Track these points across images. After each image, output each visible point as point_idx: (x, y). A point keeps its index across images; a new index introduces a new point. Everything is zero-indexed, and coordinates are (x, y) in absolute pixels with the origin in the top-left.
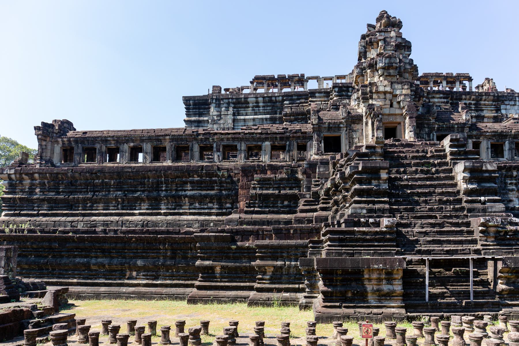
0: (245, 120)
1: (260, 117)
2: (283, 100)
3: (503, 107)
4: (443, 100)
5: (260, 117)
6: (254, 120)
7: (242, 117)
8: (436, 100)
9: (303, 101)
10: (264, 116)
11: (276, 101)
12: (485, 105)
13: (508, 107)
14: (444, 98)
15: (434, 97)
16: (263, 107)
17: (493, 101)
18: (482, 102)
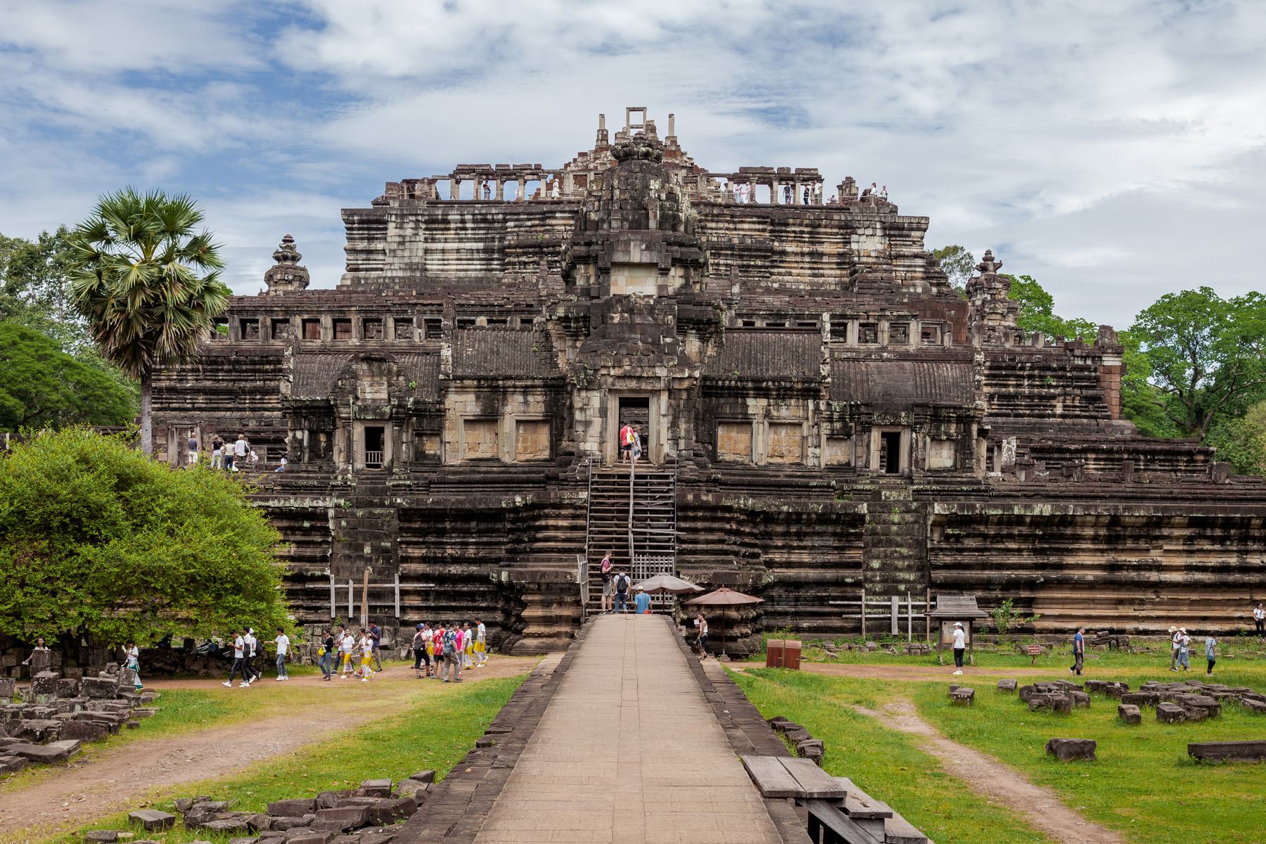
0: (443, 251)
1: (468, 245)
2: (506, 221)
3: (854, 237)
4: (757, 226)
5: (468, 245)
6: (458, 251)
7: (439, 246)
8: (746, 226)
9: (537, 222)
10: (475, 245)
11: (494, 221)
12: (826, 233)
13: (863, 238)
14: (759, 223)
15: (742, 222)
16: (473, 229)
17: (840, 227)
18: (822, 230)
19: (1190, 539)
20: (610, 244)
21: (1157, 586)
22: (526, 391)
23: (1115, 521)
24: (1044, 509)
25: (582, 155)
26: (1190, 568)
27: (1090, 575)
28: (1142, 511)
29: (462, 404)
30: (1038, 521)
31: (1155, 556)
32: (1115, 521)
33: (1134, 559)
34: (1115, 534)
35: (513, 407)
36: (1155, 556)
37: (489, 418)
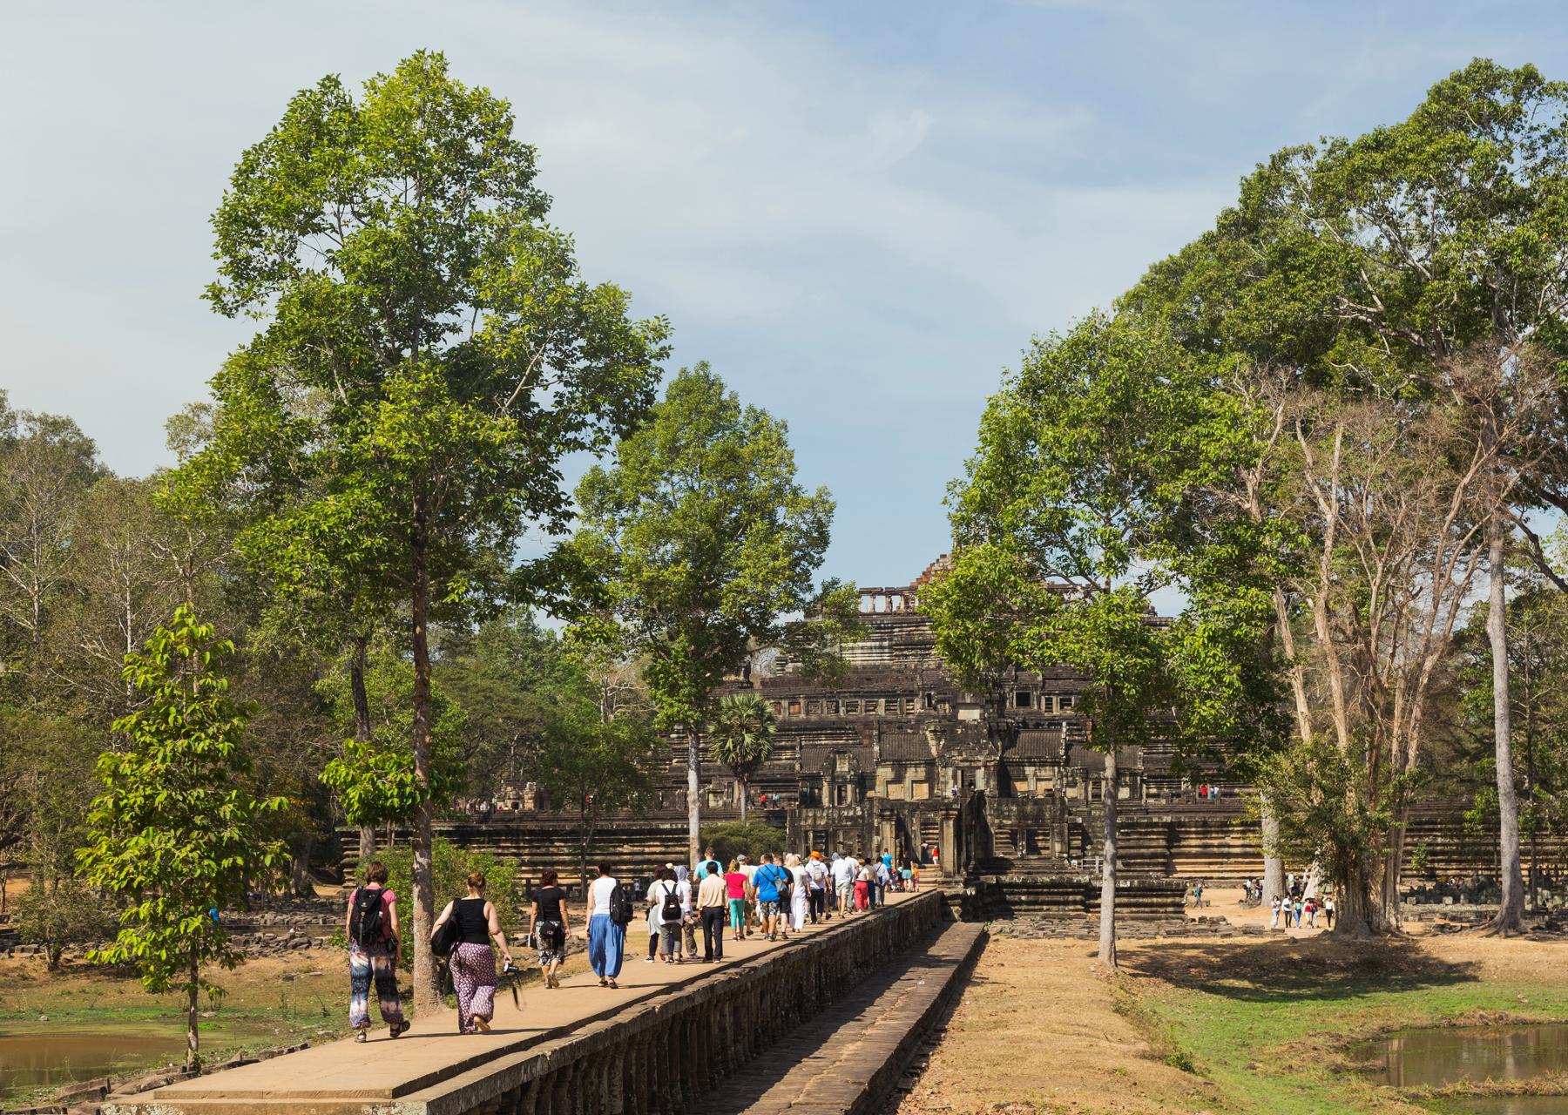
19: (1243, 832)
20: (955, 694)
21: (1228, 855)
22: (916, 766)
23: (1205, 824)
24: (1167, 819)
25: (943, 556)
26: (1243, 846)
27: (1194, 850)
28: (1219, 818)
29: (885, 773)
30: (1165, 825)
31: (1228, 840)
32: (1205, 824)
33: (1216, 842)
34: (1205, 829)
35: (910, 774)
36: (1228, 840)
37: (898, 779)
